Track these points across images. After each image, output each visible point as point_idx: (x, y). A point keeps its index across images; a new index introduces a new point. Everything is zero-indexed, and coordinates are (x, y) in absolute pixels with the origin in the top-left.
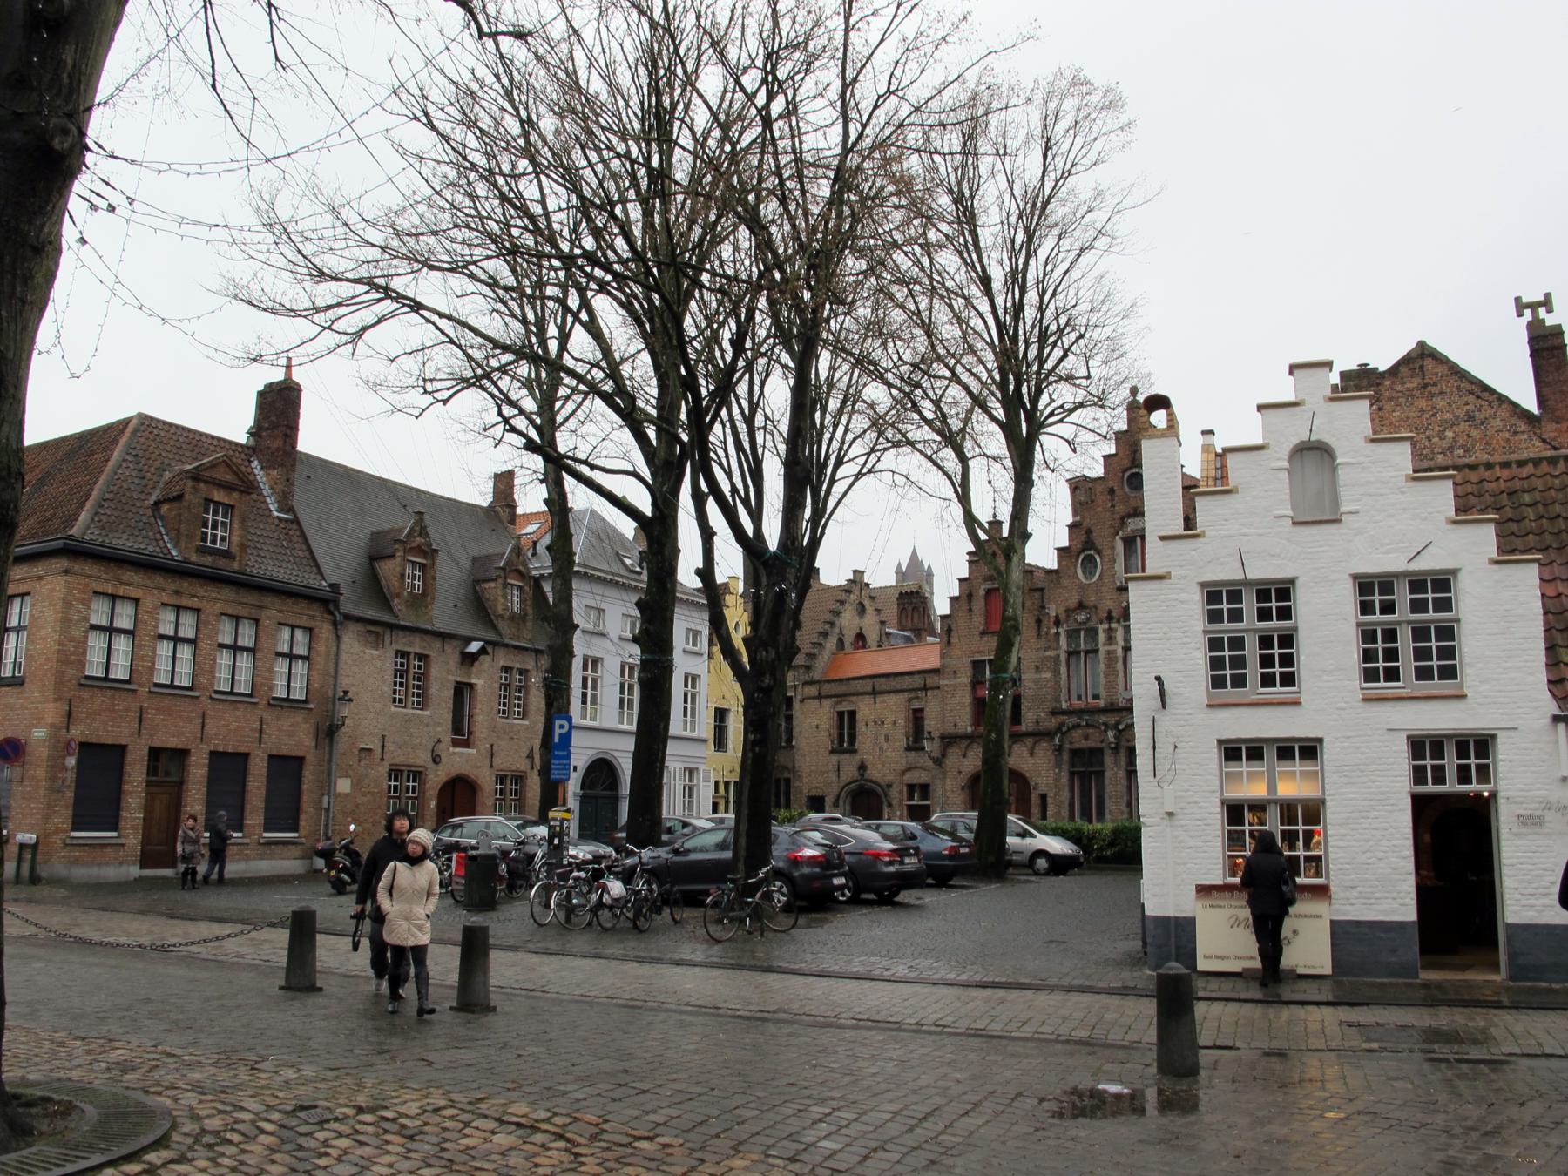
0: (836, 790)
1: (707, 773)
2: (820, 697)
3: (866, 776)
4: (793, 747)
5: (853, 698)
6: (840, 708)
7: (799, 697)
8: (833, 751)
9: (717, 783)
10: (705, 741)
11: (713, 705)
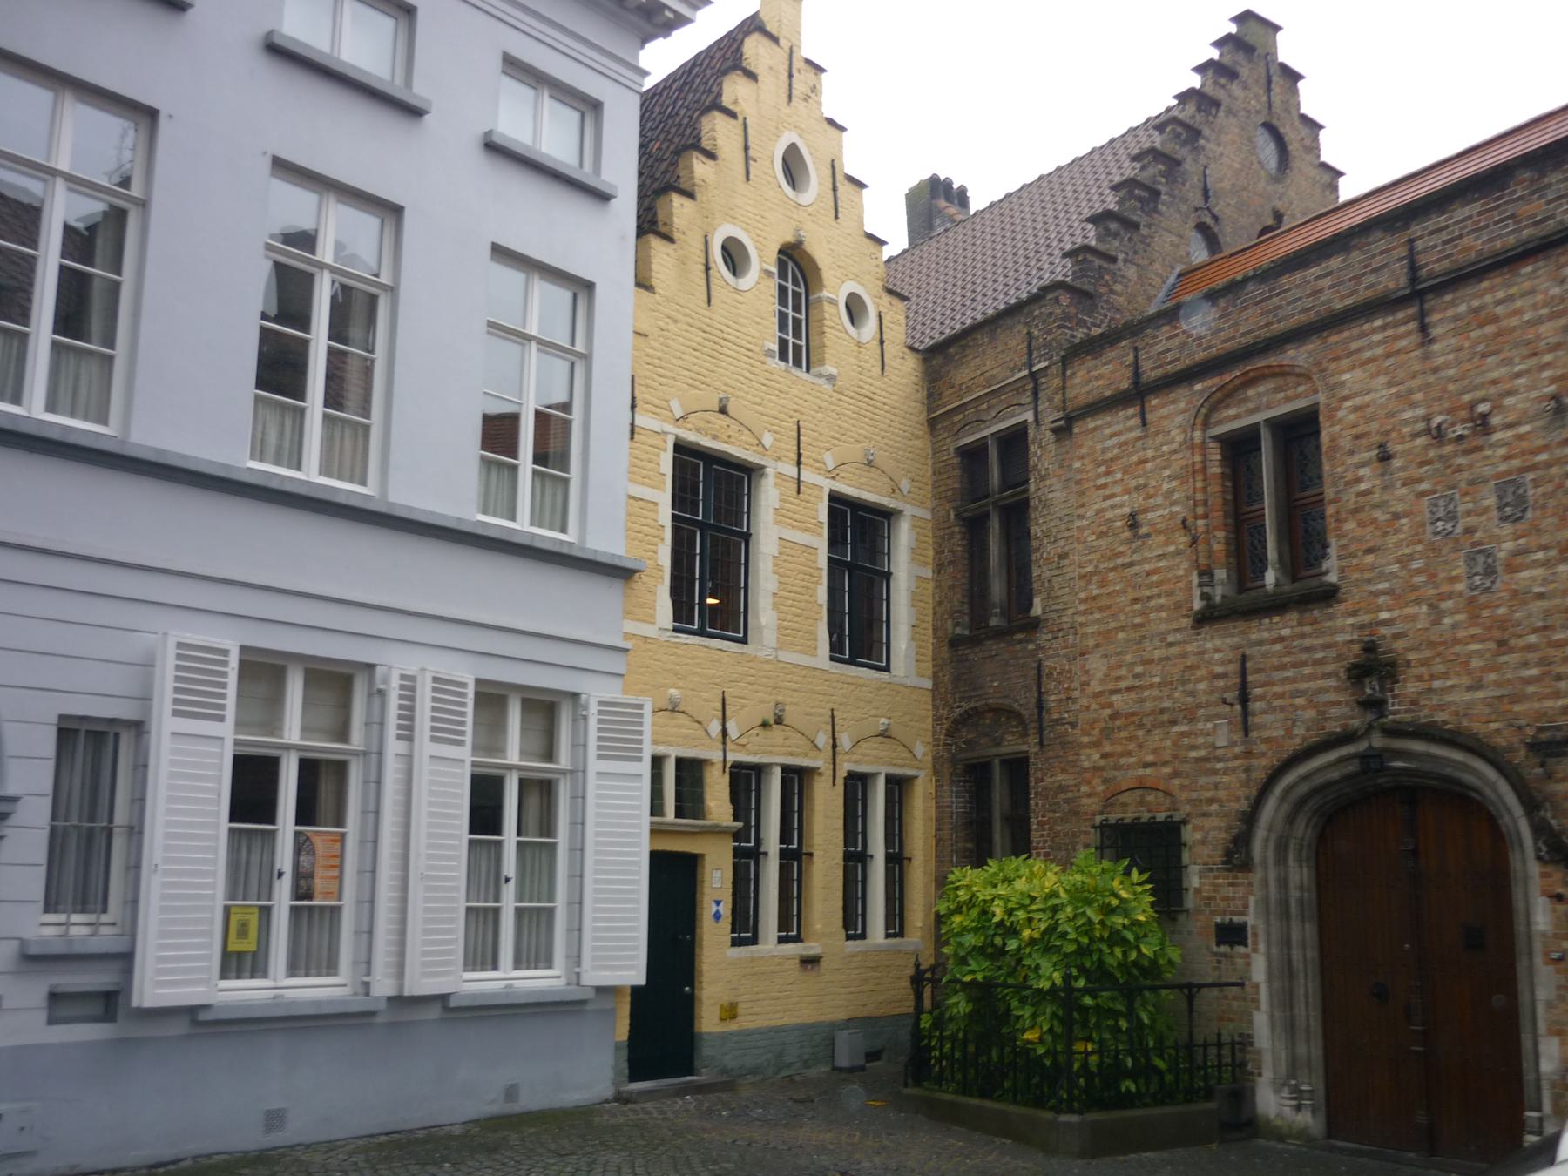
0: (1232, 790)
1: (620, 716)
2: (1138, 394)
3: (1397, 711)
4: (1034, 625)
5: (1296, 356)
6: (1234, 419)
7: (1051, 416)
8: (1208, 617)
9: (657, 762)
10: (621, 573)
11: (663, 431)
